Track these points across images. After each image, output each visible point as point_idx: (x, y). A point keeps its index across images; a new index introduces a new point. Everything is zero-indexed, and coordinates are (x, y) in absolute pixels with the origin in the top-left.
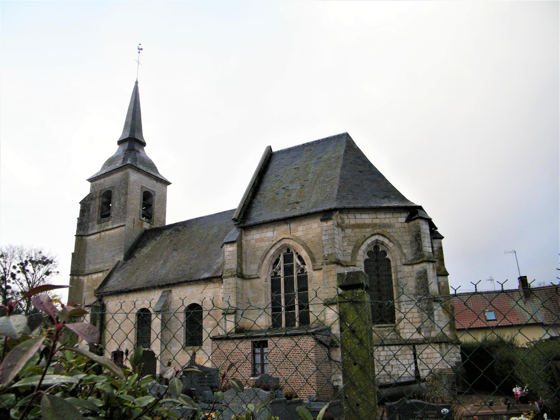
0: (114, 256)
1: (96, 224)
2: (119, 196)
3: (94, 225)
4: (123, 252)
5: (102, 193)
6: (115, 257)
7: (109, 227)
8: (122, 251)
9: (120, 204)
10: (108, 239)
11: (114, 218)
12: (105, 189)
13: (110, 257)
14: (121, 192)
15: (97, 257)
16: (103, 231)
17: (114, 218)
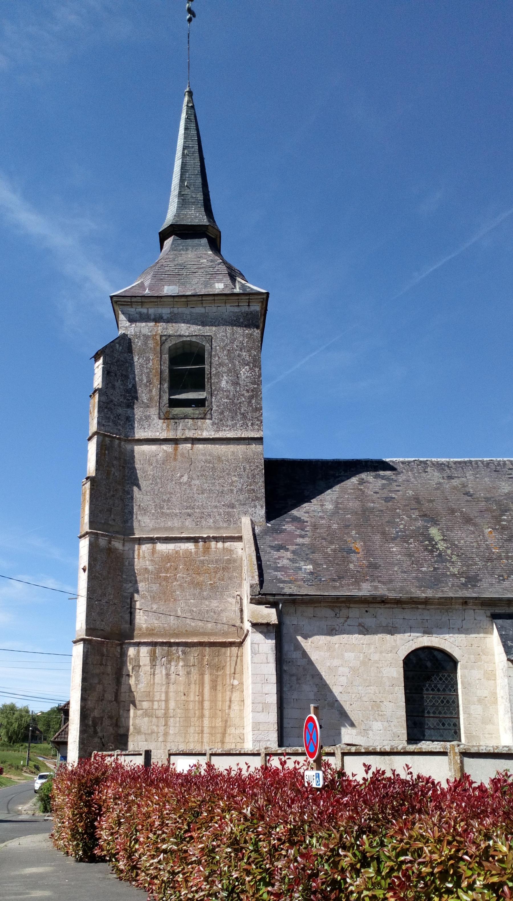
0: (233, 506)
1: (156, 417)
2: (234, 365)
3: (148, 418)
4: (263, 502)
5: (168, 345)
6: (233, 508)
7: (205, 435)
8: (257, 498)
9: (236, 384)
10: (206, 461)
11: (222, 413)
12: (180, 336)
13: (216, 507)
14: (239, 356)
15: (169, 500)
16: (186, 440)
17: (222, 413)
